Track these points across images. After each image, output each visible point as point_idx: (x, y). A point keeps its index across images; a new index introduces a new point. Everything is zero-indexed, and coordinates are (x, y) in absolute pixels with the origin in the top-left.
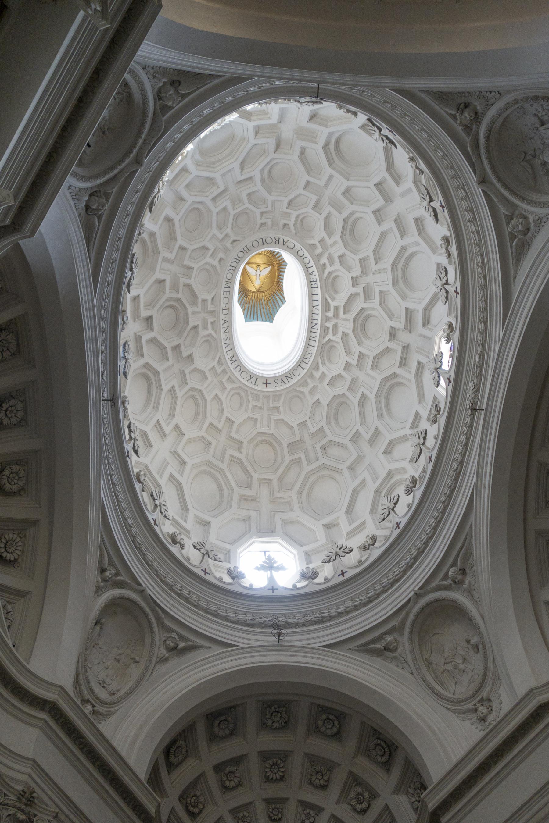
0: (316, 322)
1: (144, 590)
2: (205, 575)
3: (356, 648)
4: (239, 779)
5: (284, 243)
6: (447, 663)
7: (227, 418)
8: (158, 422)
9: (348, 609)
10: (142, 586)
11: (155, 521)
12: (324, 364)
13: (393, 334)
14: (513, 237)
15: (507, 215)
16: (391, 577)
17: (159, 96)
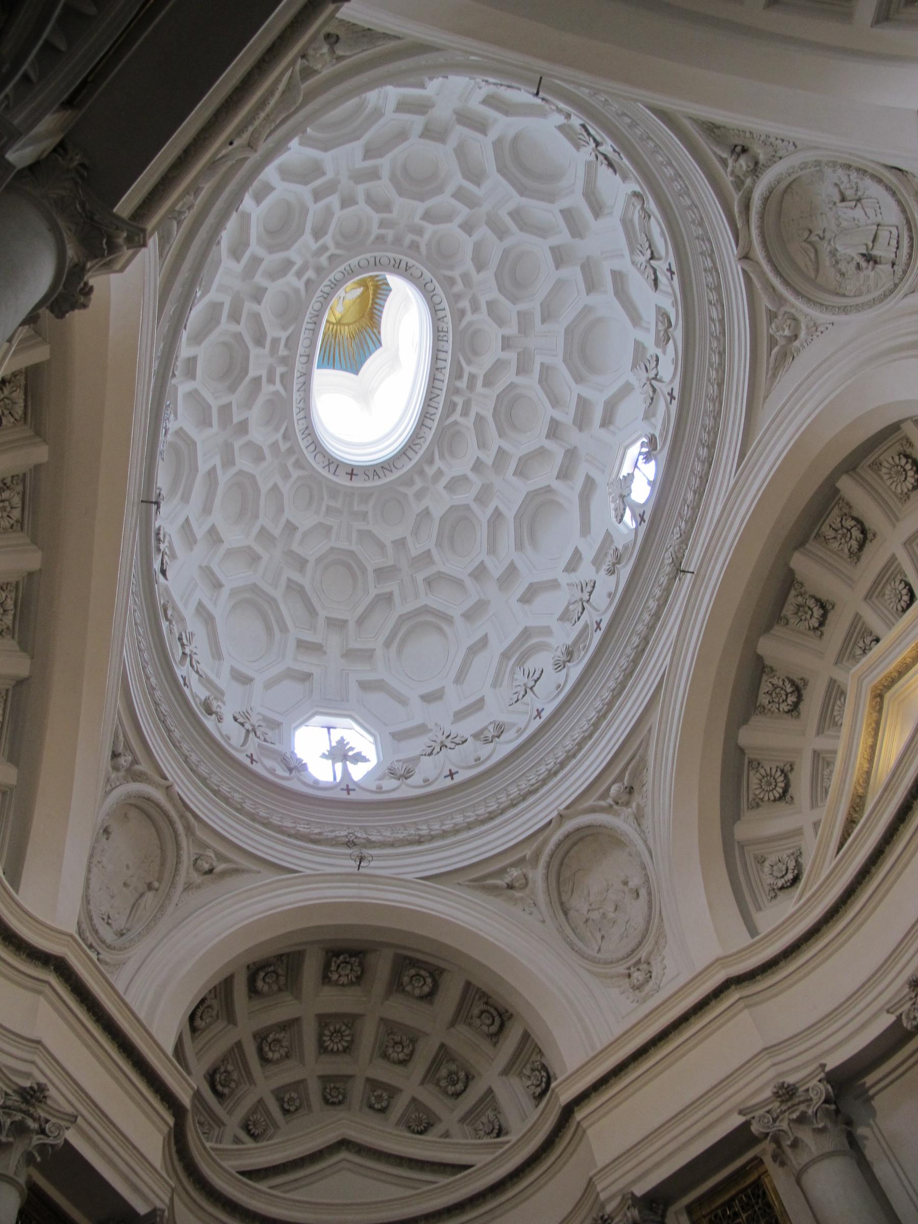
0: (438, 392)
2: (252, 763)
3: (467, 883)
4: (286, 1050)
5: (407, 268)
6: (593, 910)
7: (288, 522)
8: (187, 520)
9: (457, 827)
11: (184, 679)
12: (442, 456)
13: (554, 430)
14: (772, 341)
15: (770, 310)
16: (524, 786)
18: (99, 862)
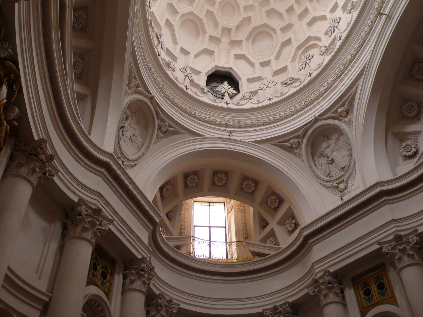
14: (135, 78)
15: (139, 87)
17: (300, 143)
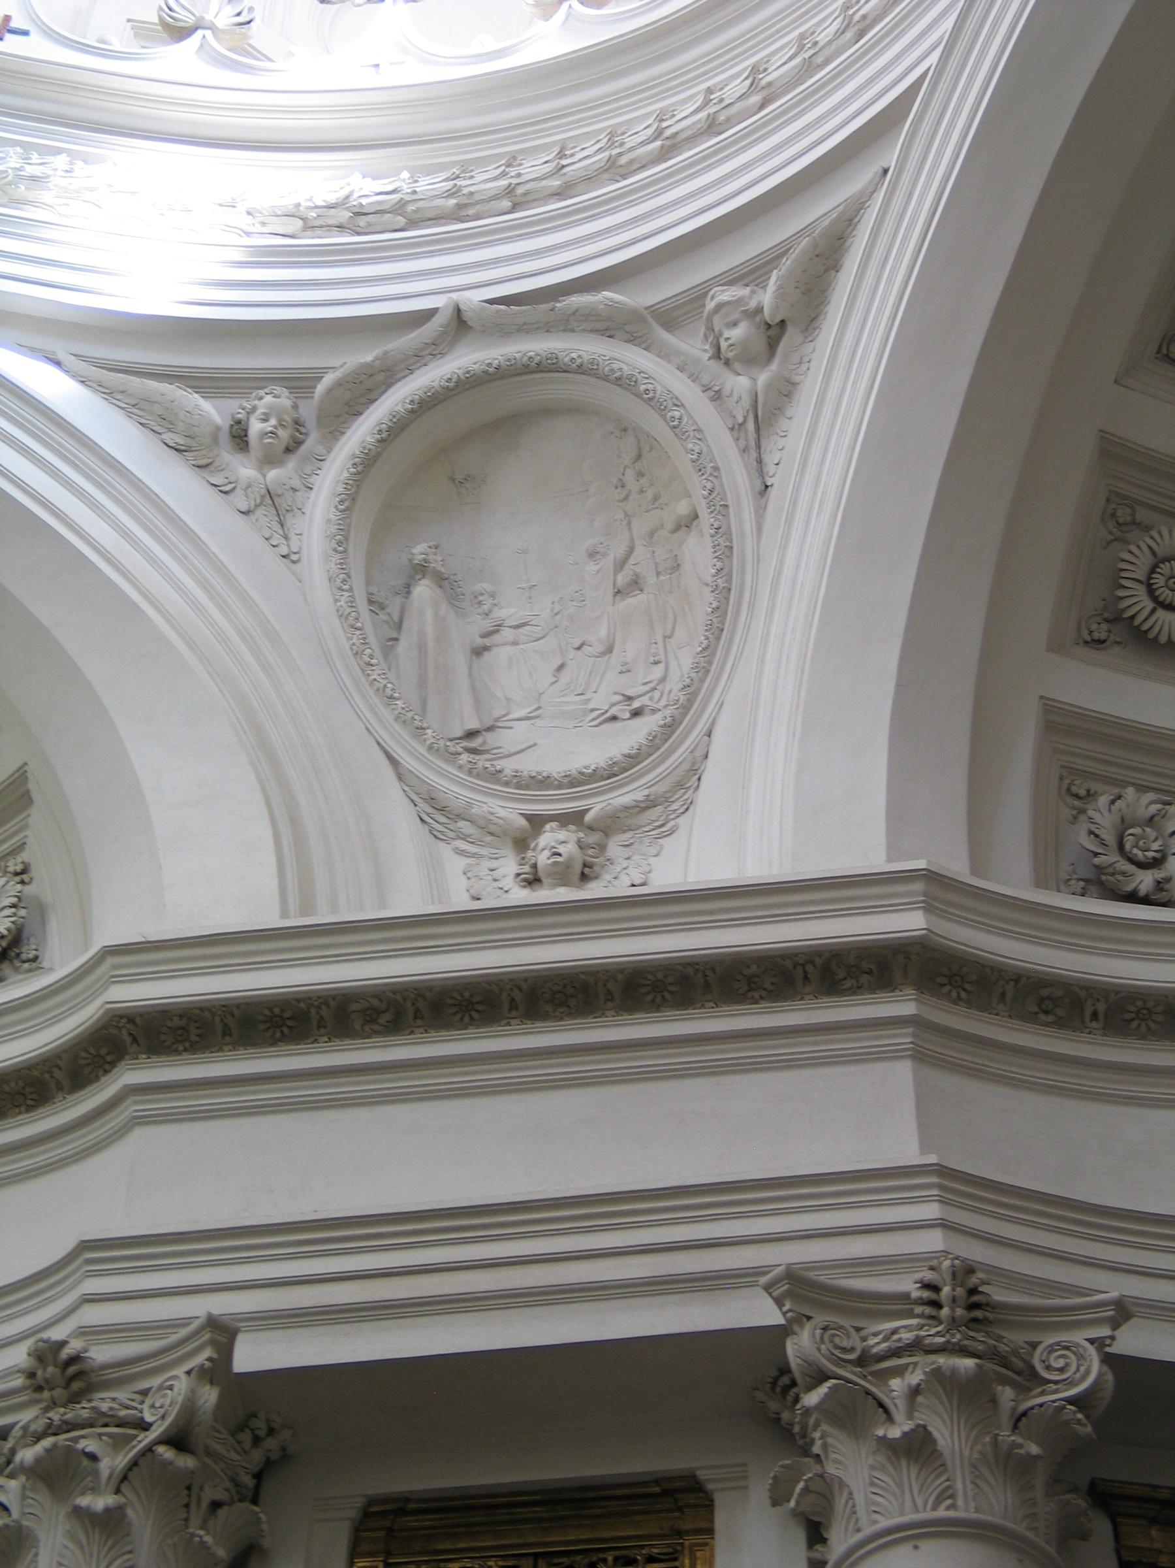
1: (458, 311)
10: (433, 312)
18: (483, 636)
